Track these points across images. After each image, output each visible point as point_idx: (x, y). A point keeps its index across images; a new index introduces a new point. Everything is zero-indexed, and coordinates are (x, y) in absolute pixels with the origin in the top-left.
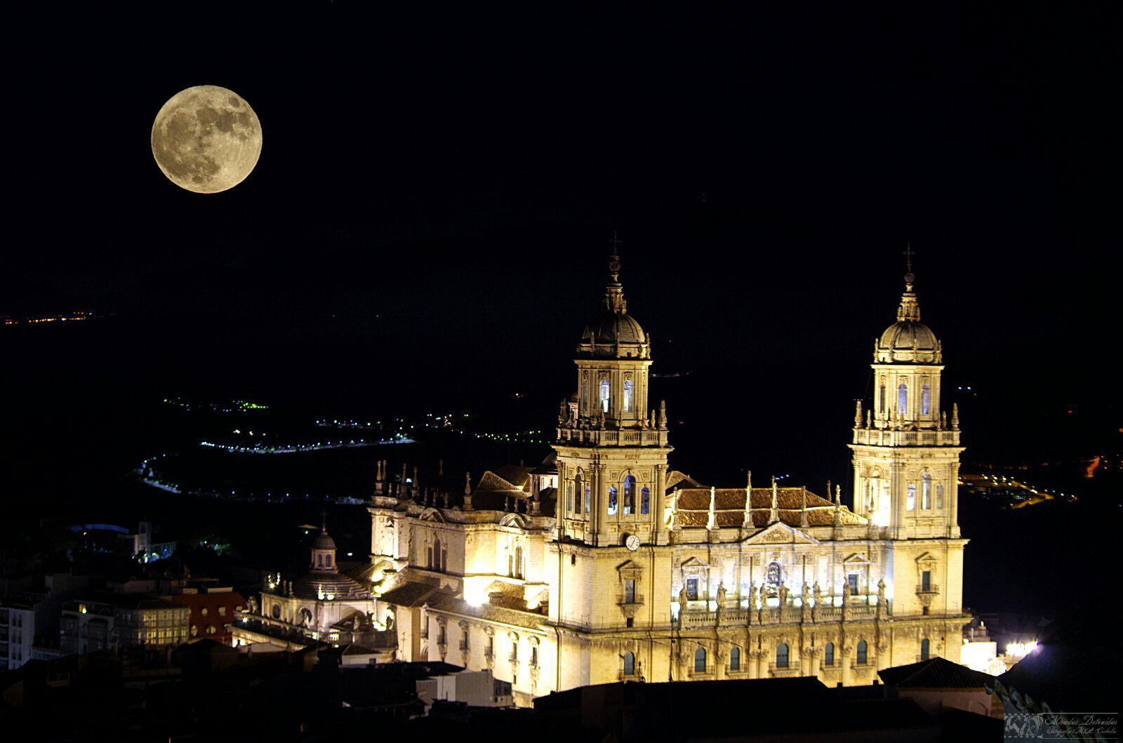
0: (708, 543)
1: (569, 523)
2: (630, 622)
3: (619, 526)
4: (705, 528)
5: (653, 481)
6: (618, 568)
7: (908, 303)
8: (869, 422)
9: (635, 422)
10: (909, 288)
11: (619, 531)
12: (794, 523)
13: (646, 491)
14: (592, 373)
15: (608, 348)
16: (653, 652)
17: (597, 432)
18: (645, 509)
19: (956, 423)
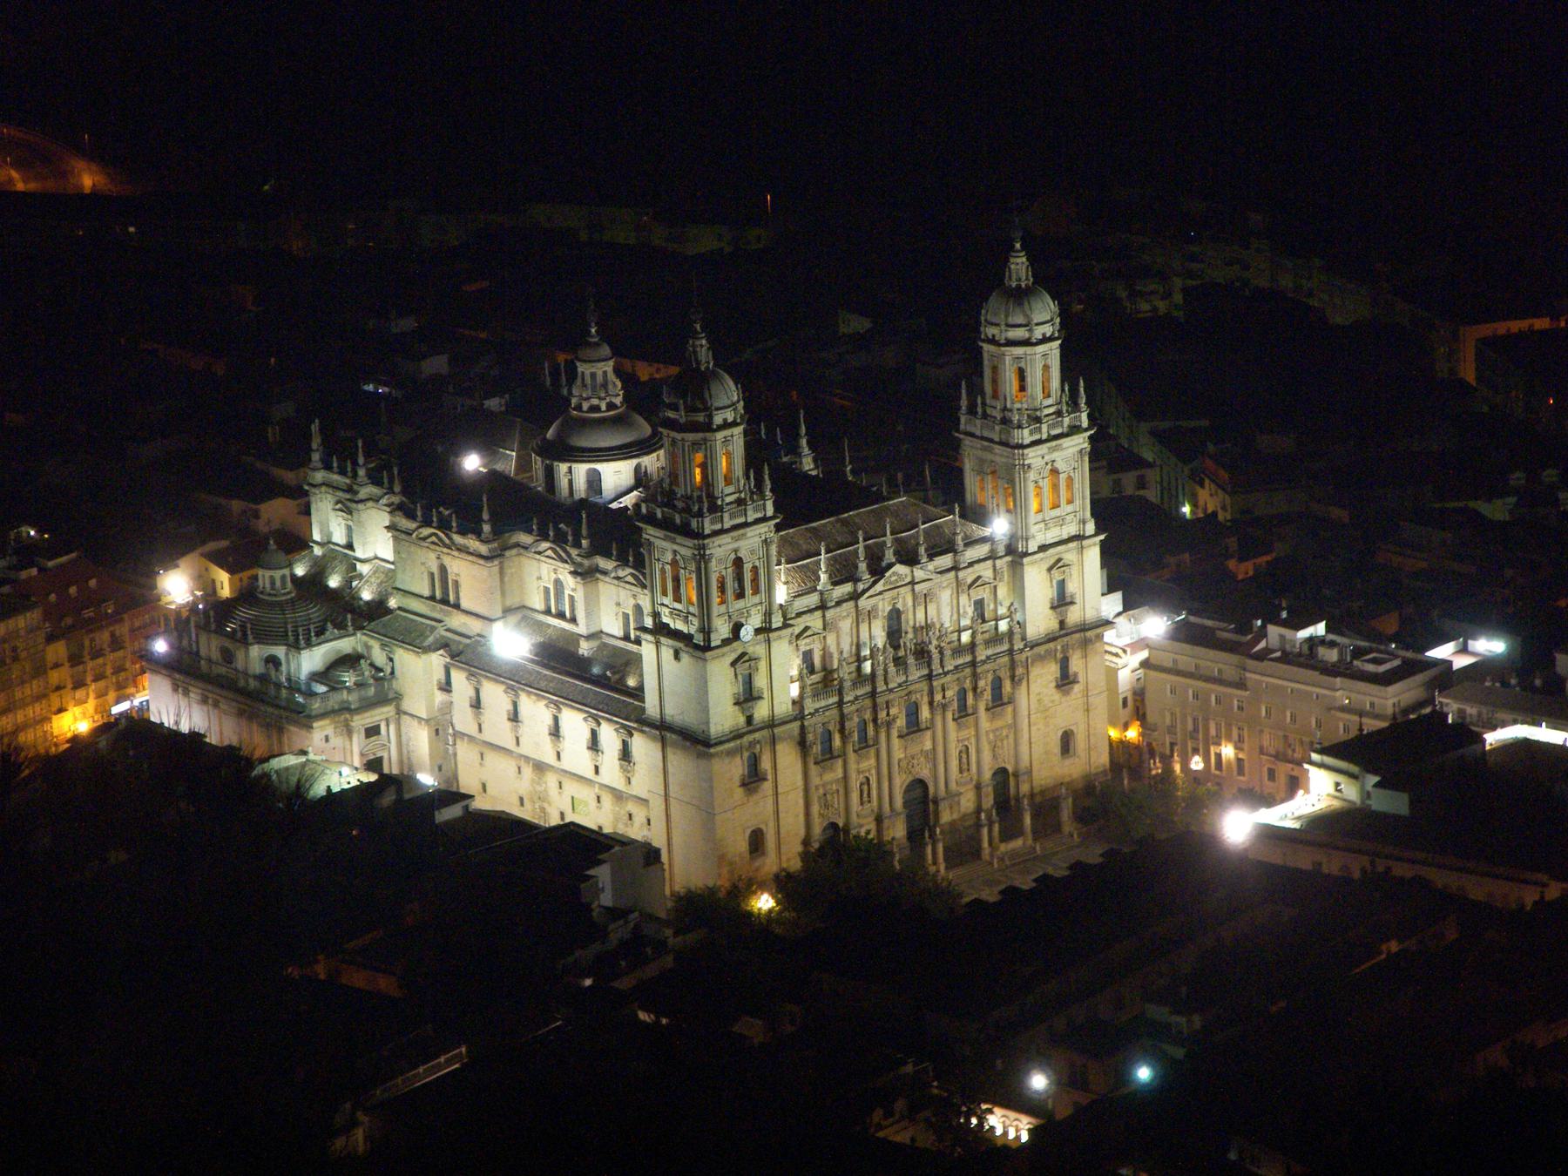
0: (823, 607)
1: (667, 611)
2: (749, 720)
3: (729, 616)
4: (816, 590)
5: (761, 556)
6: (733, 664)
7: (1019, 267)
8: (979, 410)
9: (737, 495)
10: (1018, 246)
11: (730, 622)
12: (910, 559)
13: (755, 569)
14: (683, 445)
15: (701, 417)
16: (778, 747)
17: (700, 519)
18: (756, 591)
19: (1083, 401)
